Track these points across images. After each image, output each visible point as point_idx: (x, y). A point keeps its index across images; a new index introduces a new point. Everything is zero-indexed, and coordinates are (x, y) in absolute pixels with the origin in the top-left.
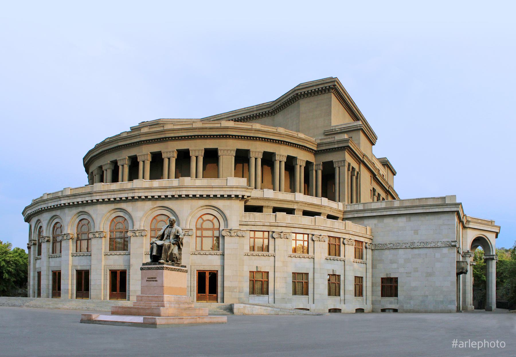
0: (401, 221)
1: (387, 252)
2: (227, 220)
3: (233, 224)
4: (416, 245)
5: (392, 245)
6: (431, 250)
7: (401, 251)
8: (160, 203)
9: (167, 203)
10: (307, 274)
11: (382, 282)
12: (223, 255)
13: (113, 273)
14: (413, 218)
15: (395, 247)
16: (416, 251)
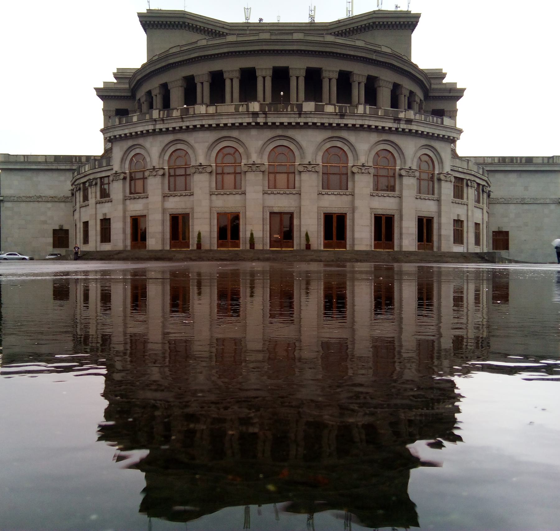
0: (513, 178)
1: (498, 206)
2: (442, 162)
3: (447, 168)
4: (526, 201)
5: (503, 200)
6: (540, 205)
7: (512, 207)
8: (385, 137)
9: (393, 138)
10: (479, 224)
11: (493, 235)
12: (439, 201)
13: (328, 218)
14: (524, 175)
15: (507, 202)
16: (526, 207)
